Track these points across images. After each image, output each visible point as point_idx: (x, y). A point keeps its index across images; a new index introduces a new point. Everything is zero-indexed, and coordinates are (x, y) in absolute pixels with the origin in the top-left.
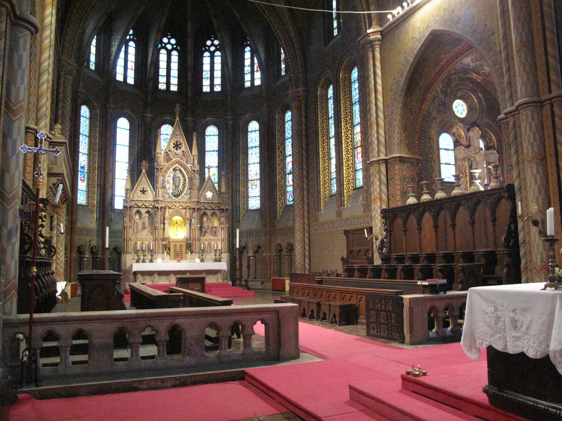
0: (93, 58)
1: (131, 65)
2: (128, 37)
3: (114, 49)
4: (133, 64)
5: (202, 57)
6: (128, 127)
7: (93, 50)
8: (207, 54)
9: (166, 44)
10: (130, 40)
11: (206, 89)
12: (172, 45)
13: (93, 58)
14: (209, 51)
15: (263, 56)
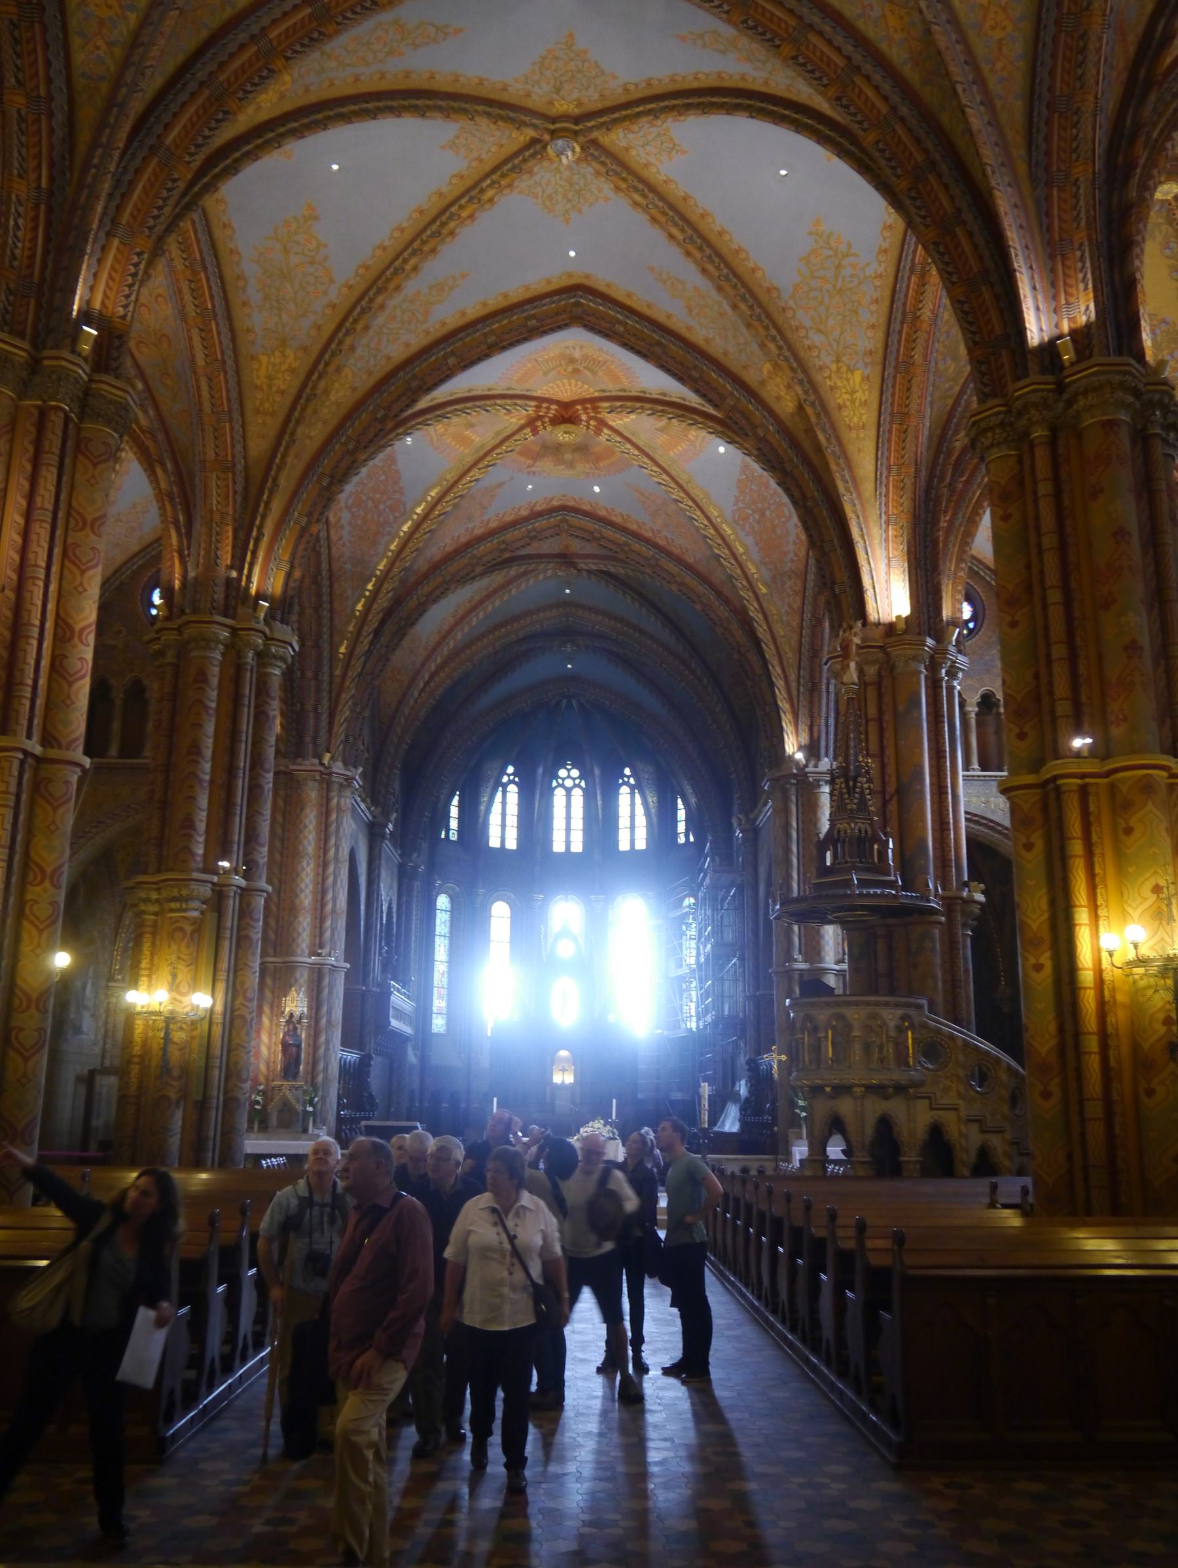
0: (454, 824)
1: (512, 821)
2: (505, 779)
3: (482, 808)
4: (515, 819)
5: (617, 794)
6: (509, 915)
7: (454, 812)
8: (625, 790)
9: (563, 779)
10: (510, 782)
11: (624, 845)
12: (574, 779)
13: (454, 824)
14: (627, 784)
15: (693, 800)
